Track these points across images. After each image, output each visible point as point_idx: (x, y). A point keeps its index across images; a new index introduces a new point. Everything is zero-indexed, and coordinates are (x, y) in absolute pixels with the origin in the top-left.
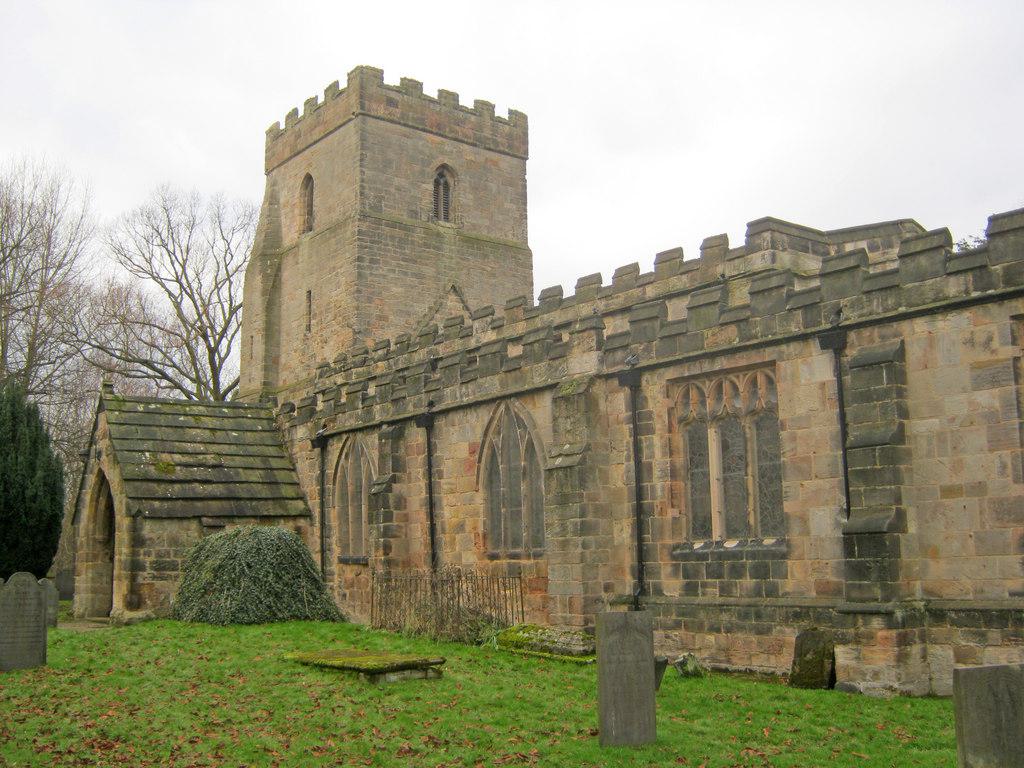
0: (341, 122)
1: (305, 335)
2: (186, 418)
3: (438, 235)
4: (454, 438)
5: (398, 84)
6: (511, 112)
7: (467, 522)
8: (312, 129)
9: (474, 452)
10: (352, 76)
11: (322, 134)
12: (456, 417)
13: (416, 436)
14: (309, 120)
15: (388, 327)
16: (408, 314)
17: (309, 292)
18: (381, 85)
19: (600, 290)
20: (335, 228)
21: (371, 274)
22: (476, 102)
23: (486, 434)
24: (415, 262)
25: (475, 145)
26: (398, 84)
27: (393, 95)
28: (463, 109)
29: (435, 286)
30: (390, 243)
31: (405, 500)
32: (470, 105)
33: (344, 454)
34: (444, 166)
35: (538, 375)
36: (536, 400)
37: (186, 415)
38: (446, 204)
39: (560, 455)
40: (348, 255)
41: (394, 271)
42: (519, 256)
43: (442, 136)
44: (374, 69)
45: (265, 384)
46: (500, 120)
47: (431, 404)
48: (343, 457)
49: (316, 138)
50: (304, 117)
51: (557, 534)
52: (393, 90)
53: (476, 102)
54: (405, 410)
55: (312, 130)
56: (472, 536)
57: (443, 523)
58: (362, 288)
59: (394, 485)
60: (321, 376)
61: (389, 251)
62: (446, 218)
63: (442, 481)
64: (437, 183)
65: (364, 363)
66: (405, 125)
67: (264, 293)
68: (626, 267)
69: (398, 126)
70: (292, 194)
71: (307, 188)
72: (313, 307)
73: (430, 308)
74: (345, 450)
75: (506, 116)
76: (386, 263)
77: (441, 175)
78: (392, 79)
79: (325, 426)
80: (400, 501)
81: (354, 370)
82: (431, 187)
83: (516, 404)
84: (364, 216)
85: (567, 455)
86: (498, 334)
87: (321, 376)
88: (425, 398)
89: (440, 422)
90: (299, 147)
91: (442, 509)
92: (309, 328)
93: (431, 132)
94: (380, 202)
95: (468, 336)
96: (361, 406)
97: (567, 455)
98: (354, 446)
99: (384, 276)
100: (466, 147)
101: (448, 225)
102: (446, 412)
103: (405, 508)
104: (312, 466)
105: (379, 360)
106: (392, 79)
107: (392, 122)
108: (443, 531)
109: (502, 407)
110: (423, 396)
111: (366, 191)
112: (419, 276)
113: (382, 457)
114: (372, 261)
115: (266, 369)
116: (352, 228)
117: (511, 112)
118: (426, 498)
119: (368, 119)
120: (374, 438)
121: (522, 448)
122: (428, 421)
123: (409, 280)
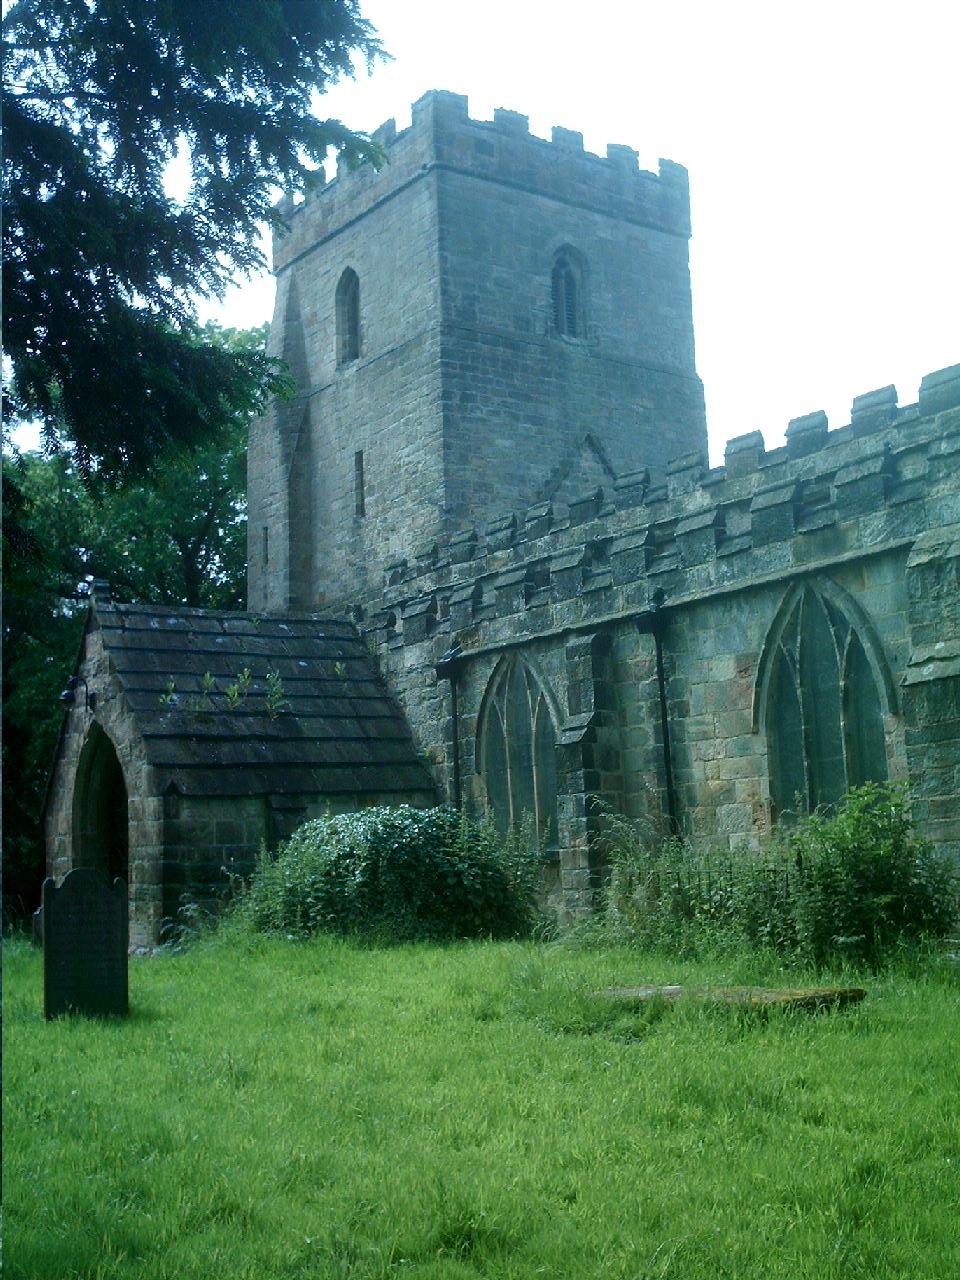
0: (402, 182)
1: (355, 522)
2: (227, 639)
3: (561, 355)
4: (708, 647)
5: (491, 119)
6: (662, 162)
7: (738, 785)
8: (353, 197)
9: (746, 670)
10: (419, 107)
11: (372, 204)
12: (713, 616)
13: (640, 652)
14: (347, 185)
15: (493, 501)
16: (522, 480)
17: (359, 455)
18: (466, 120)
19: (895, 413)
20: (399, 352)
21: (464, 418)
22: (610, 147)
23: (770, 640)
24: (528, 398)
25: (610, 214)
26: (491, 119)
27: (484, 135)
28: (592, 158)
29: (561, 436)
30: (491, 369)
31: (617, 753)
32: (602, 153)
33: (496, 685)
34: (565, 249)
35: (869, 534)
36: (865, 575)
37: (225, 634)
38: (572, 308)
39: (931, 659)
40: (425, 390)
41: (497, 413)
42: (680, 397)
43: (560, 199)
44: (454, 96)
45: (291, 600)
46: (647, 175)
47: (659, 596)
48: (495, 690)
49: (358, 212)
50: (337, 180)
51: (933, 791)
52: (483, 128)
53: (610, 147)
54: (610, 607)
55: (353, 198)
56: (749, 807)
57: (689, 790)
58: (456, 440)
59: (600, 731)
60: (393, 581)
61: (490, 381)
62: (573, 333)
63: (688, 720)
64: (555, 276)
65: (471, 554)
66: (505, 183)
67: (286, 457)
68: (878, 392)
69: (495, 186)
70: (323, 305)
71: (346, 293)
72: (367, 477)
73: (555, 472)
74: (498, 679)
75: (655, 169)
76: (486, 400)
77: (561, 263)
78: (481, 111)
79: (456, 644)
80: (608, 753)
81: (454, 568)
82: (547, 280)
83: (827, 590)
84: (448, 328)
85: (942, 659)
86: (712, 496)
87: (393, 581)
88: (649, 588)
89: (683, 623)
90: (331, 227)
91: (688, 765)
92: (361, 510)
93: (544, 194)
94: (473, 305)
95: (659, 501)
96: (523, 606)
97: (942, 659)
98: (513, 672)
99: (483, 421)
100: (598, 217)
101: (574, 340)
102: (691, 607)
103: (618, 767)
104: (435, 710)
105: (498, 548)
106: (481, 111)
107: (485, 178)
108: (692, 802)
109: (800, 593)
110: (646, 584)
111: (451, 288)
112: (535, 420)
113: (574, 689)
114: (465, 398)
115: (292, 577)
116: (431, 346)
117: (662, 162)
118: (656, 749)
119: (451, 174)
120: (555, 657)
121: (841, 661)
122: (662, 625)
123: (524, 427)
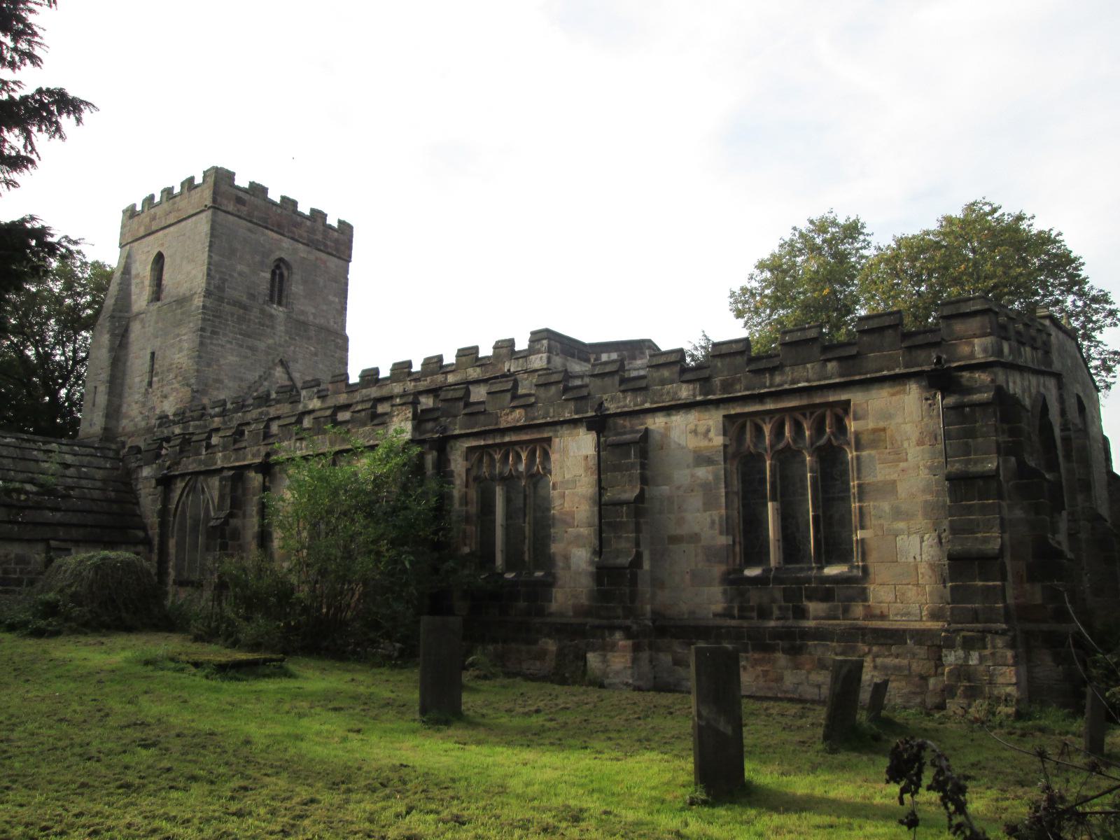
0: (192, 212)
3: (272, 316)
6: (340, 222)
8: (168, 214)
13: (256, 479)
16: (241, 380)
19: (410, 374)
24: (249, 337)
27: (241, 194)
28: (301, 215)
32: (307, 212)
34: (281, 260)
38: (281, 291)
41: (231, 343)
44: (228, 171)
46: (330, 227)
47: (268, 455)
49: (169, 222)
58: (202, 353)
62: (280, 304)
64: (273, 273)
66: (251, 222)
67: (111, 350)
69: (244, 222)
70: (143, 269)
72: (156, 366)
73: (260, 377)
75: (335, 225)
76: (225, 335)
77: (278, 267)
78: (242, 181)
79: (169, 468)
81: (192, 423)
82: (268, 275)
84: (208, 293)
86: (322, 402)
88: (263, 450)
90: (154, 228)
91: (272, 541)
92: (150, 384)
93: (272, 230)
99: (222, 346)
100: (301, 245)
101: (281, 309)
103: (239, 539)
104: (154, 501)
106: (242, 181)
107: (239, 217)
111: (213, 273)
112: (253, 349)
113: (222, 497)
114: (213, 333)
115: (108, 416)
117: (340, 222)
119: (219, 212)
120: (215, 482)
122: (266, 468)
